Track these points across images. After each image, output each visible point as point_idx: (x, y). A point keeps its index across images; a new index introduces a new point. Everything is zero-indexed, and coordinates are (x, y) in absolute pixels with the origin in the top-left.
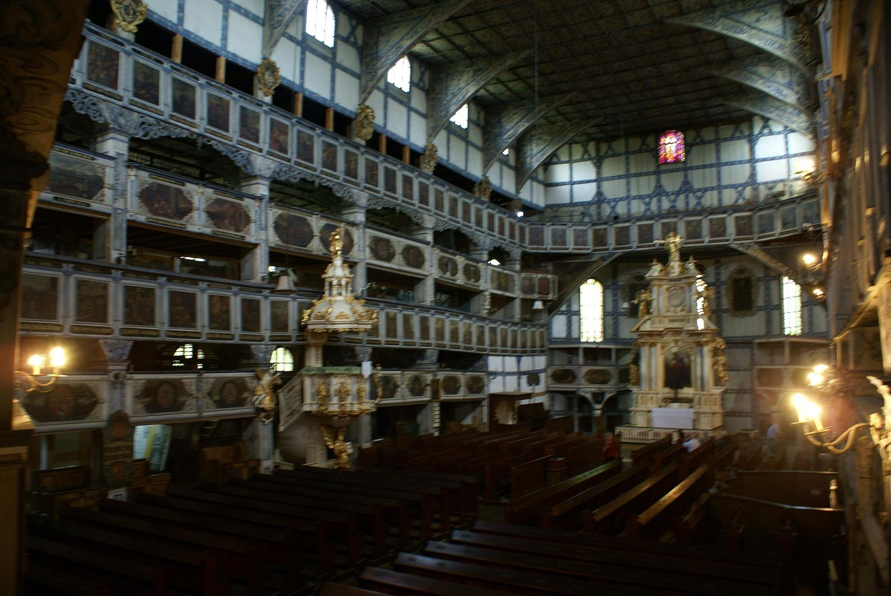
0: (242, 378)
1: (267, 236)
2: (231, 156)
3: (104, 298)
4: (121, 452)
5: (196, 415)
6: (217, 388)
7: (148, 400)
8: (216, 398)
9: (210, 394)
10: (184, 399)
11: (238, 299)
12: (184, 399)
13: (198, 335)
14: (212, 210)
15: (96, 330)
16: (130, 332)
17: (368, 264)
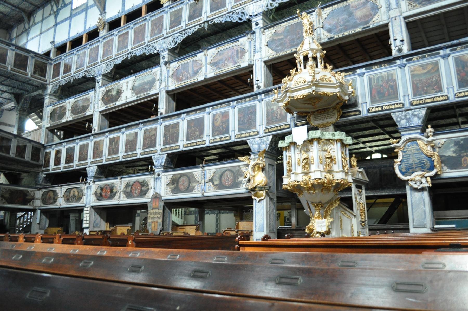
0: (239, 166)
1: (261, 55)
2: (229, 20)
3: (155, 135)
4: (156, 216)
5: (200, 195)
6: (218, 176)
7: (174, 186)
8: (216, 183)
9: (211, 180)
10: (194, 184)
11: (236, 109)
12: (194, 184)
13: (204, 143)
14: (215, 61)
15: (151, 152)
16: (165, 150)
17: (405, 18)
